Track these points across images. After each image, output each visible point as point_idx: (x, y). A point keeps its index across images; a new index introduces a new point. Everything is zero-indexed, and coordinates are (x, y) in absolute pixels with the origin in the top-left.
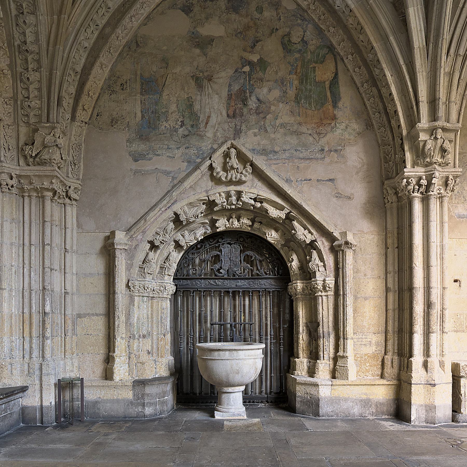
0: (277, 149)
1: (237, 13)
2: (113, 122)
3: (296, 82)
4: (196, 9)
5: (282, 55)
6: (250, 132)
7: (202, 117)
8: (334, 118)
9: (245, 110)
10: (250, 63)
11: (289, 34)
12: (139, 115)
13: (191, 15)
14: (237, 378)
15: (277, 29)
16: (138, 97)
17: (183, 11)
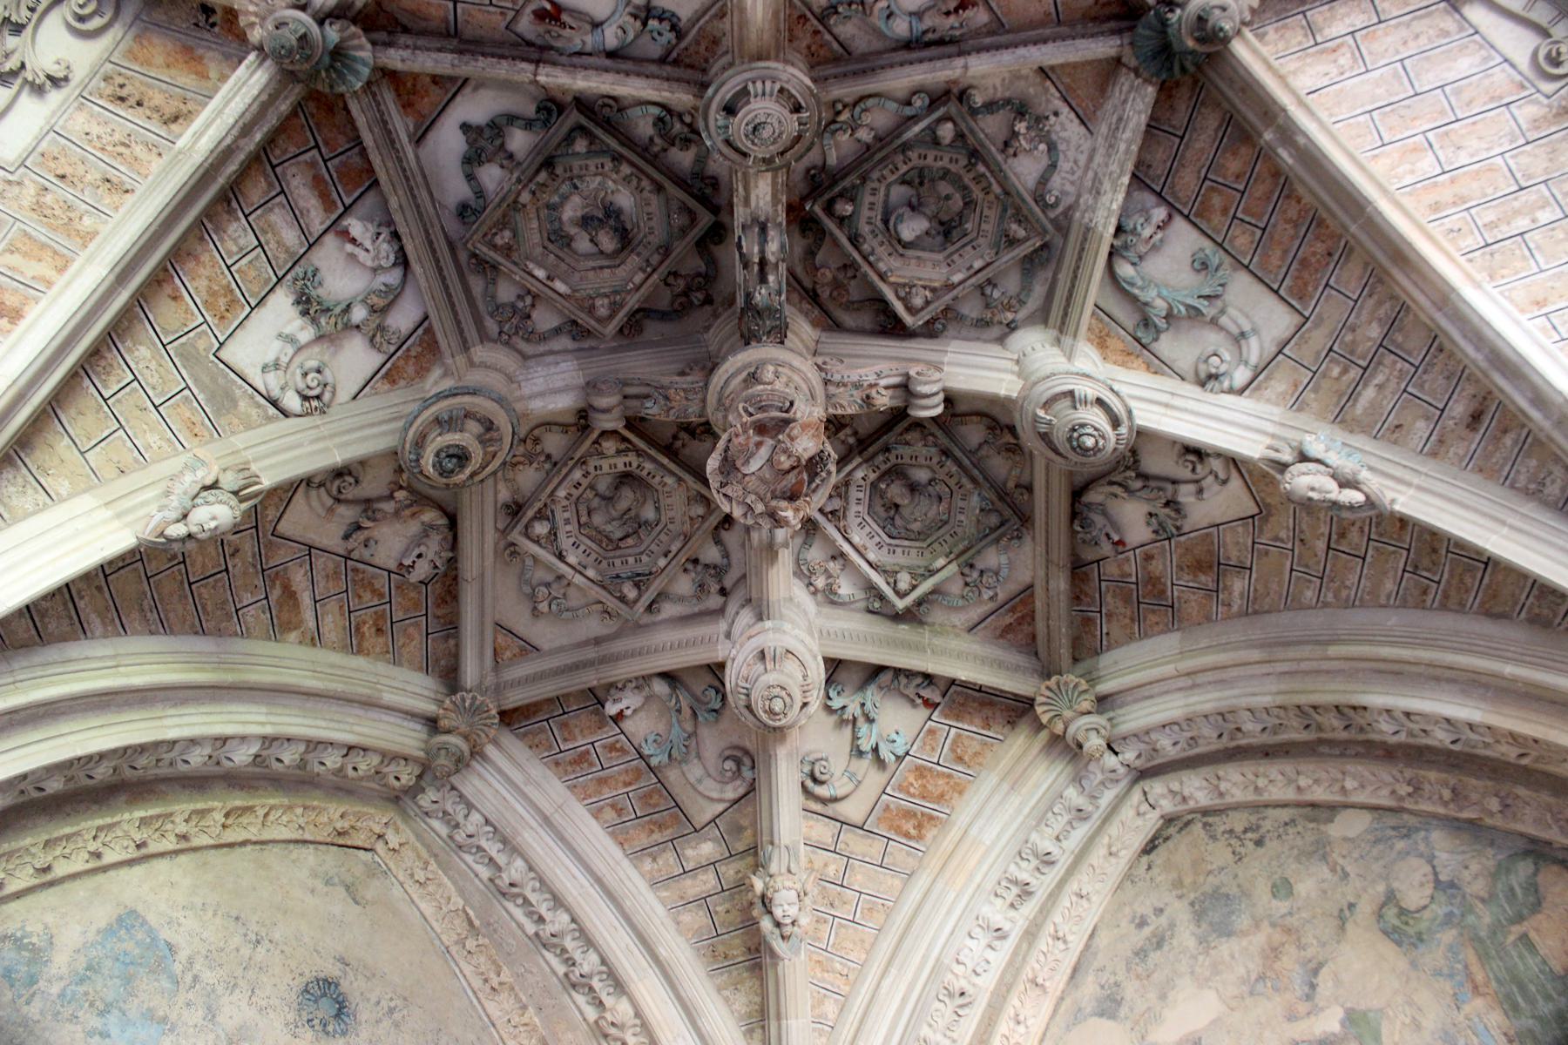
1: (1230, 934)
4: (1130, 990)
5: (1402, 964)
11: (1391, 897)
13: (1123, 1011)
15: (1351, 906)
17: (1101, 1015)
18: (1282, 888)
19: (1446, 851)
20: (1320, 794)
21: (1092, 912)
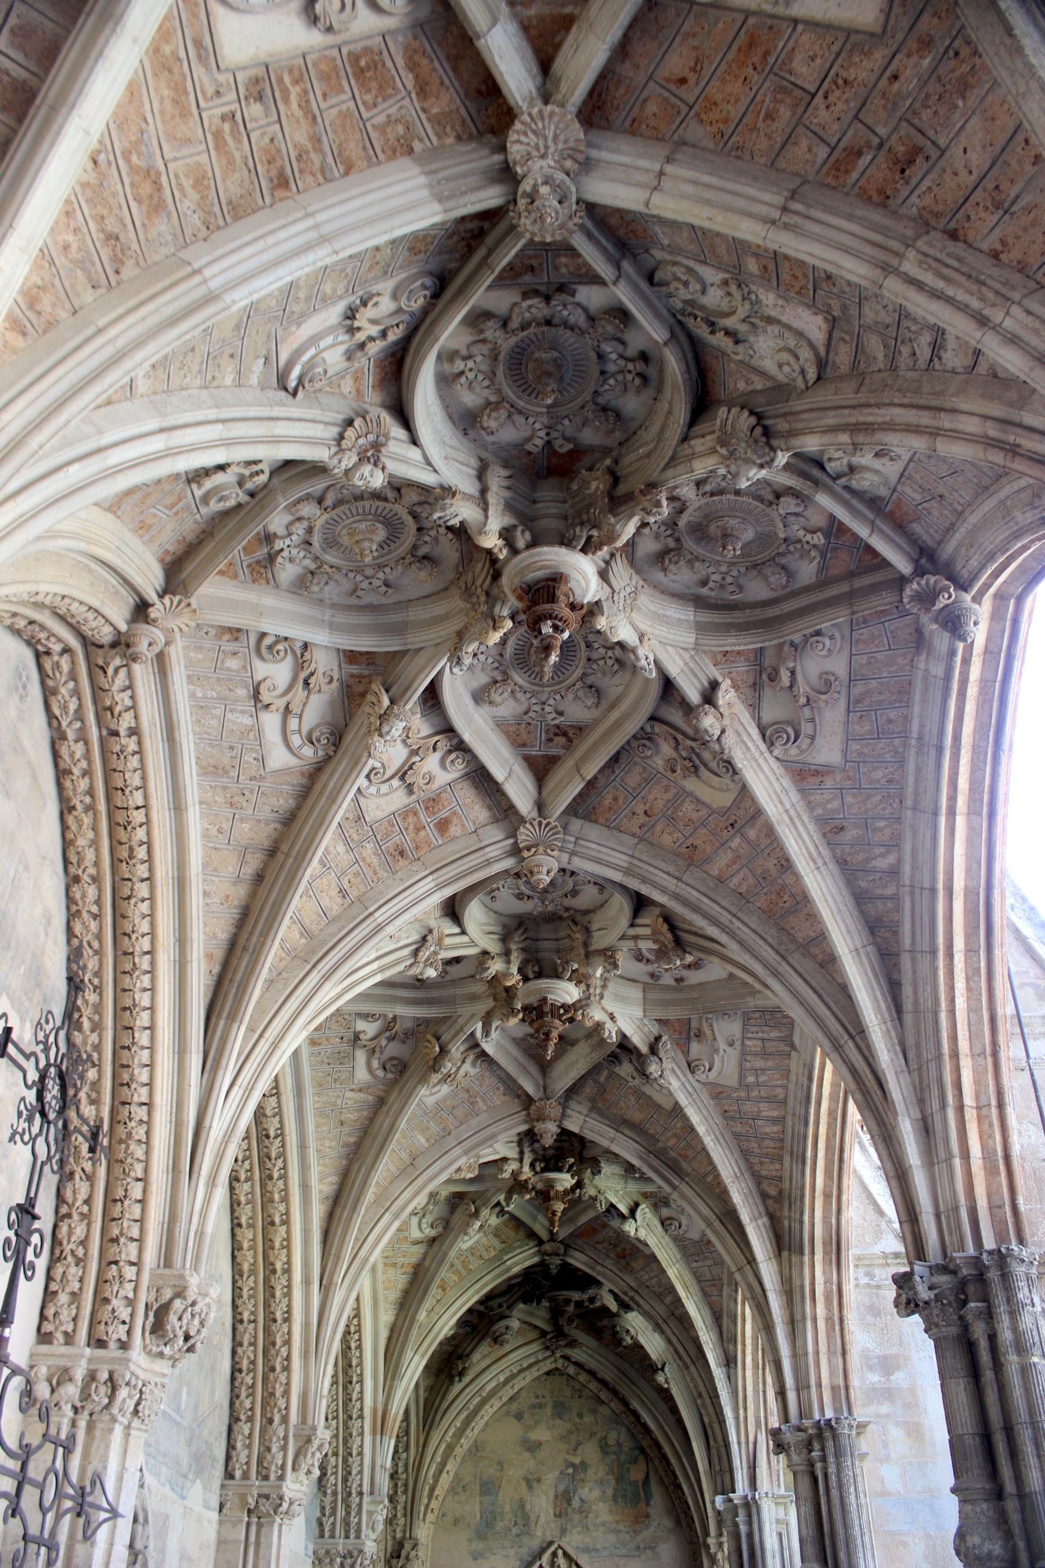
0: (598, 1546)
2: (456, 1522)
3: (613, 1482)
4: (526, 1416)
6: (575, 1531)
7: (533, 1517)
8: (648, 1516)
9: (570, 1510)
10: (573, 1465)
11: (605, 1438)
12: (478, 1515)
16: (478, 1498)
18: (580, 1415)
19: (624, 1435)
20: (603, 1397)
21: (523, 1383)
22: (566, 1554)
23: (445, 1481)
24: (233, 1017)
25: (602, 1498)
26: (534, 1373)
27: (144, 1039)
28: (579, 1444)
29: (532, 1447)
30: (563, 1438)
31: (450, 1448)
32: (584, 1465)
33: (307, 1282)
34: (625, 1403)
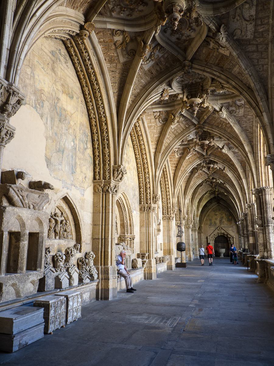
2: (207, 224)
14: (222, 252)
18: (222, 211)
22: (221, 228)
23: (205, 219)
24: (186, 195)
25: (226, 221)
26: (216, 206)
27: (180, 199)
28: (222, 214)
29: (216, 215)
30: (220, 214)
31: (205, 215)
32: (223, 217)
33: (190, 207)
34: (228, 209)
